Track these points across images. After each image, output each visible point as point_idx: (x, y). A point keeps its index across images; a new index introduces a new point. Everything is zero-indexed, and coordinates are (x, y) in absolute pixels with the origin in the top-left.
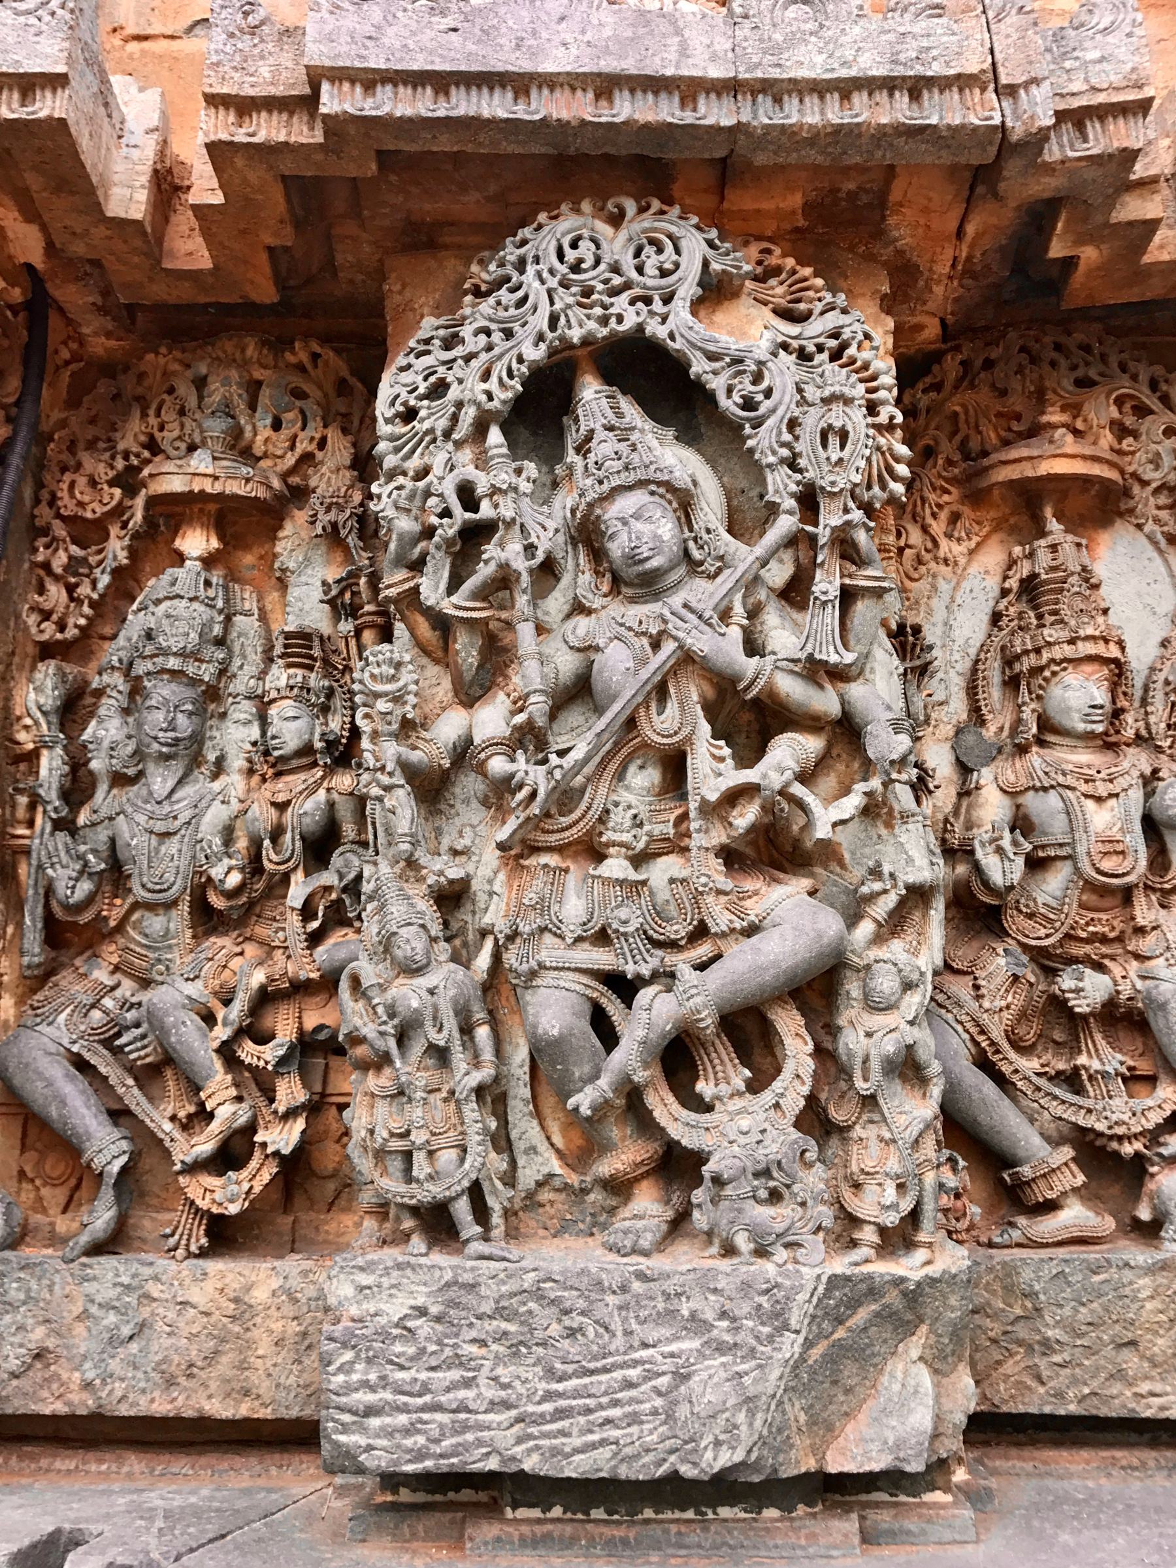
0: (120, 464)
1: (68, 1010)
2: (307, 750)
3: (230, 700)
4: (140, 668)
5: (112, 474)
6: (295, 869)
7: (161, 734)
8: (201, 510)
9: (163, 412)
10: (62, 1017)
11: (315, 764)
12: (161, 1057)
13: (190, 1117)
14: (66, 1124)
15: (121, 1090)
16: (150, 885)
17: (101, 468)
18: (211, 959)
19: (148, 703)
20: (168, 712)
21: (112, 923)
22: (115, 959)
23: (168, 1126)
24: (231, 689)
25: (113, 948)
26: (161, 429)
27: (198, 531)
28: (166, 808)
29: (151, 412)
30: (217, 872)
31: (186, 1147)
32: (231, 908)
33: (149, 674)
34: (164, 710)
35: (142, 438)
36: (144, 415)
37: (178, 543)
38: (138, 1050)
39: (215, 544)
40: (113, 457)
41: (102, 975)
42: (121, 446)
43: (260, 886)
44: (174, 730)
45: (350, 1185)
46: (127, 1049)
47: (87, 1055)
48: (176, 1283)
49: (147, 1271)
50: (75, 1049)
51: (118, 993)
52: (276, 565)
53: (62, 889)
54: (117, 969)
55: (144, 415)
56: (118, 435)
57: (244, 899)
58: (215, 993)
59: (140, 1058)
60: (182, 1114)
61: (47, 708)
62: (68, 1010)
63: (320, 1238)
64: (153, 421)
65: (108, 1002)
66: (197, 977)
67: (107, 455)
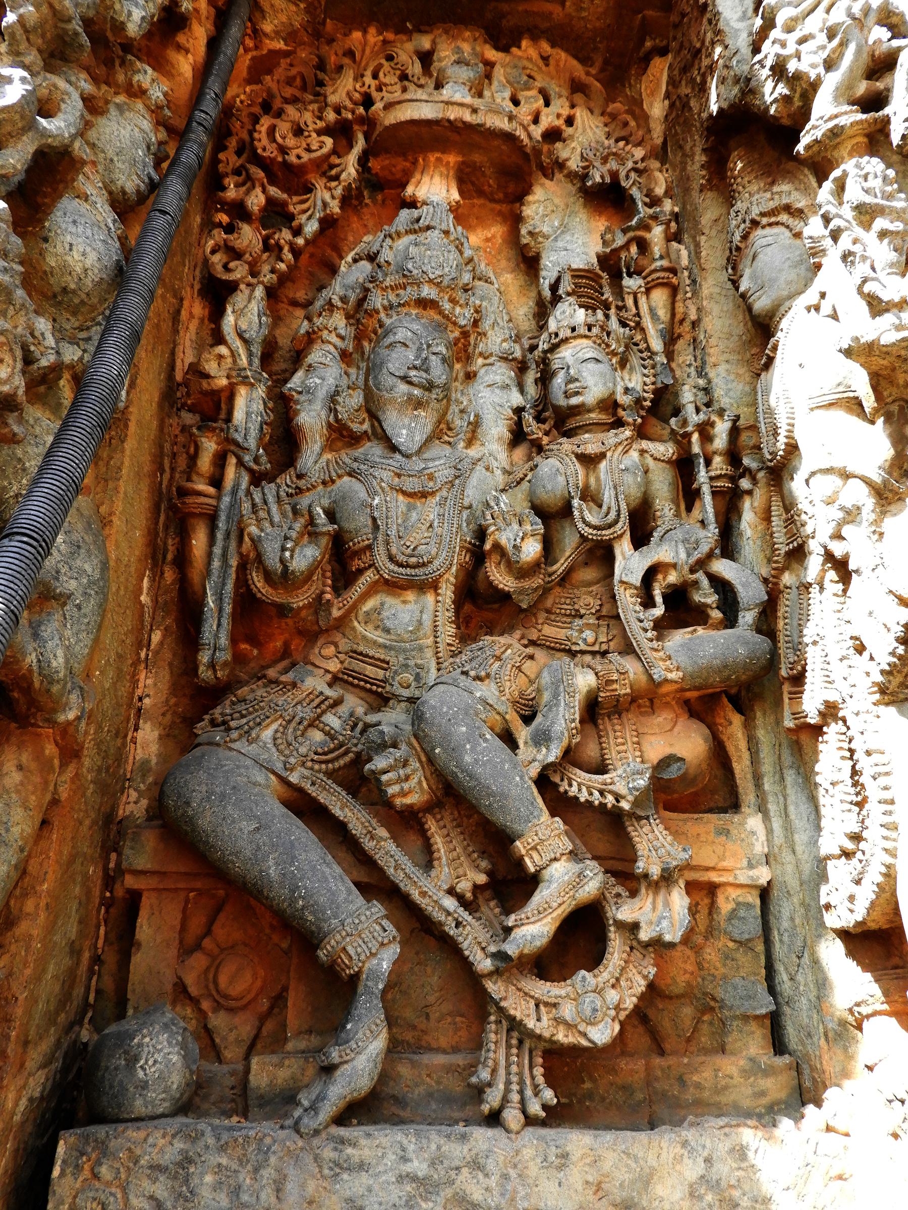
0: (331, 116)
1: (275, 726)
2: (610, 405)
3: (480, 361)
4: (377, 300)
5: (321, 124)
6: (621, 536)
7: (413, 373)
8: (438, 160)
9: (381, 75)
10: (267, 734)
11: (619, 423)
12: (426, 797)
13: (476, 888)
14: (294, 889)
15: (368, 845)
16: (401, 558)
17: (308, 117)
18: (499, 658)
19: (390, 339)
20: (420, 349)
21: (336, 613)
22: (334, 666)
23: (450, 903)
24: (481, 347)
25: (330, 650)
26: (379, 89)
27: (437, 179)
28: (417, 464)
29: (368, 73)
30: (506, 537)
31: (483, 936)
32: (522, 591)
33: (389, 307)
34: (414, 348)
35: (357, 96)
36: (359, 77)
37: (410, 190)
38: (399, 780)
39: (455, 196)
40: (321, 110)
41: (316, 683)
42: (333, 99)
43: (560, 567)
44: (427, 371)
45: (712, 1009)
46: (384, 778)
47: (312, 790)
48: (513, 1173)
49: (457, 1151)
50: (294, 778)
51: (343, 710)
52: (523, 231)
53: (272, 560)
54: (335, 680)
55: (359, 77)
56: (329, 90)
57: (537, 581)
58: (514, 702)
59: (403, 793)
60: (464, 886)
61: (252, 334)
62: (275, 726)
63: (689, 1095)
64: (368, 80)
65: (332, 721)
66: (488, 676)
67: (315, 106)
